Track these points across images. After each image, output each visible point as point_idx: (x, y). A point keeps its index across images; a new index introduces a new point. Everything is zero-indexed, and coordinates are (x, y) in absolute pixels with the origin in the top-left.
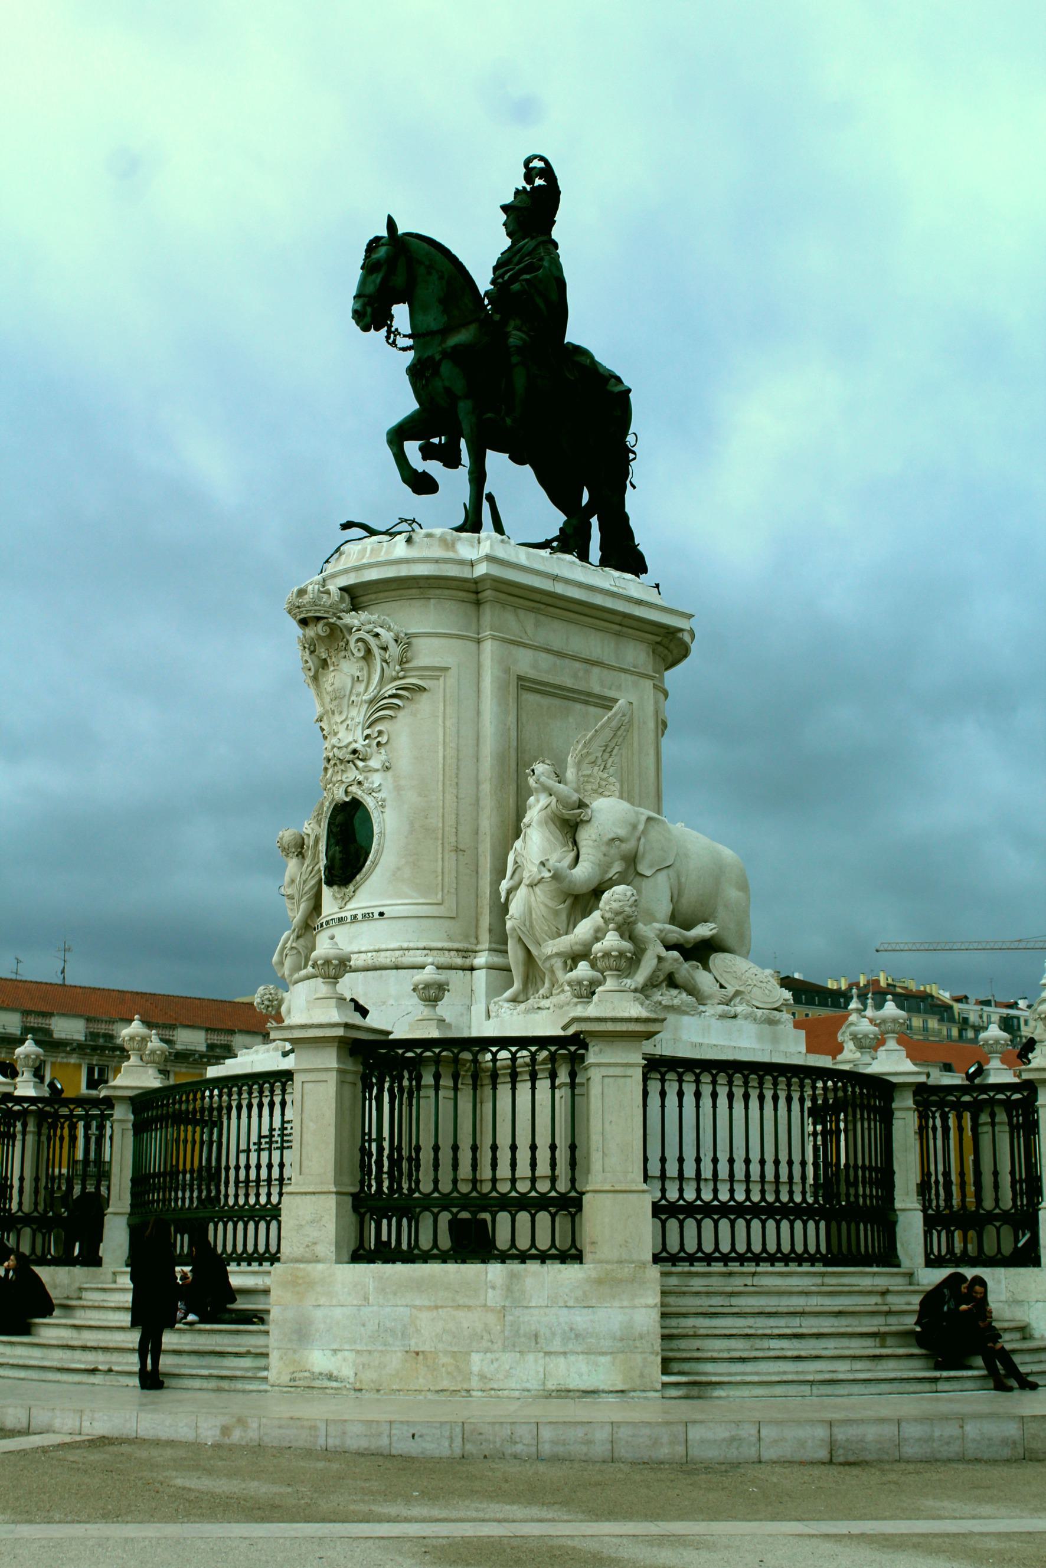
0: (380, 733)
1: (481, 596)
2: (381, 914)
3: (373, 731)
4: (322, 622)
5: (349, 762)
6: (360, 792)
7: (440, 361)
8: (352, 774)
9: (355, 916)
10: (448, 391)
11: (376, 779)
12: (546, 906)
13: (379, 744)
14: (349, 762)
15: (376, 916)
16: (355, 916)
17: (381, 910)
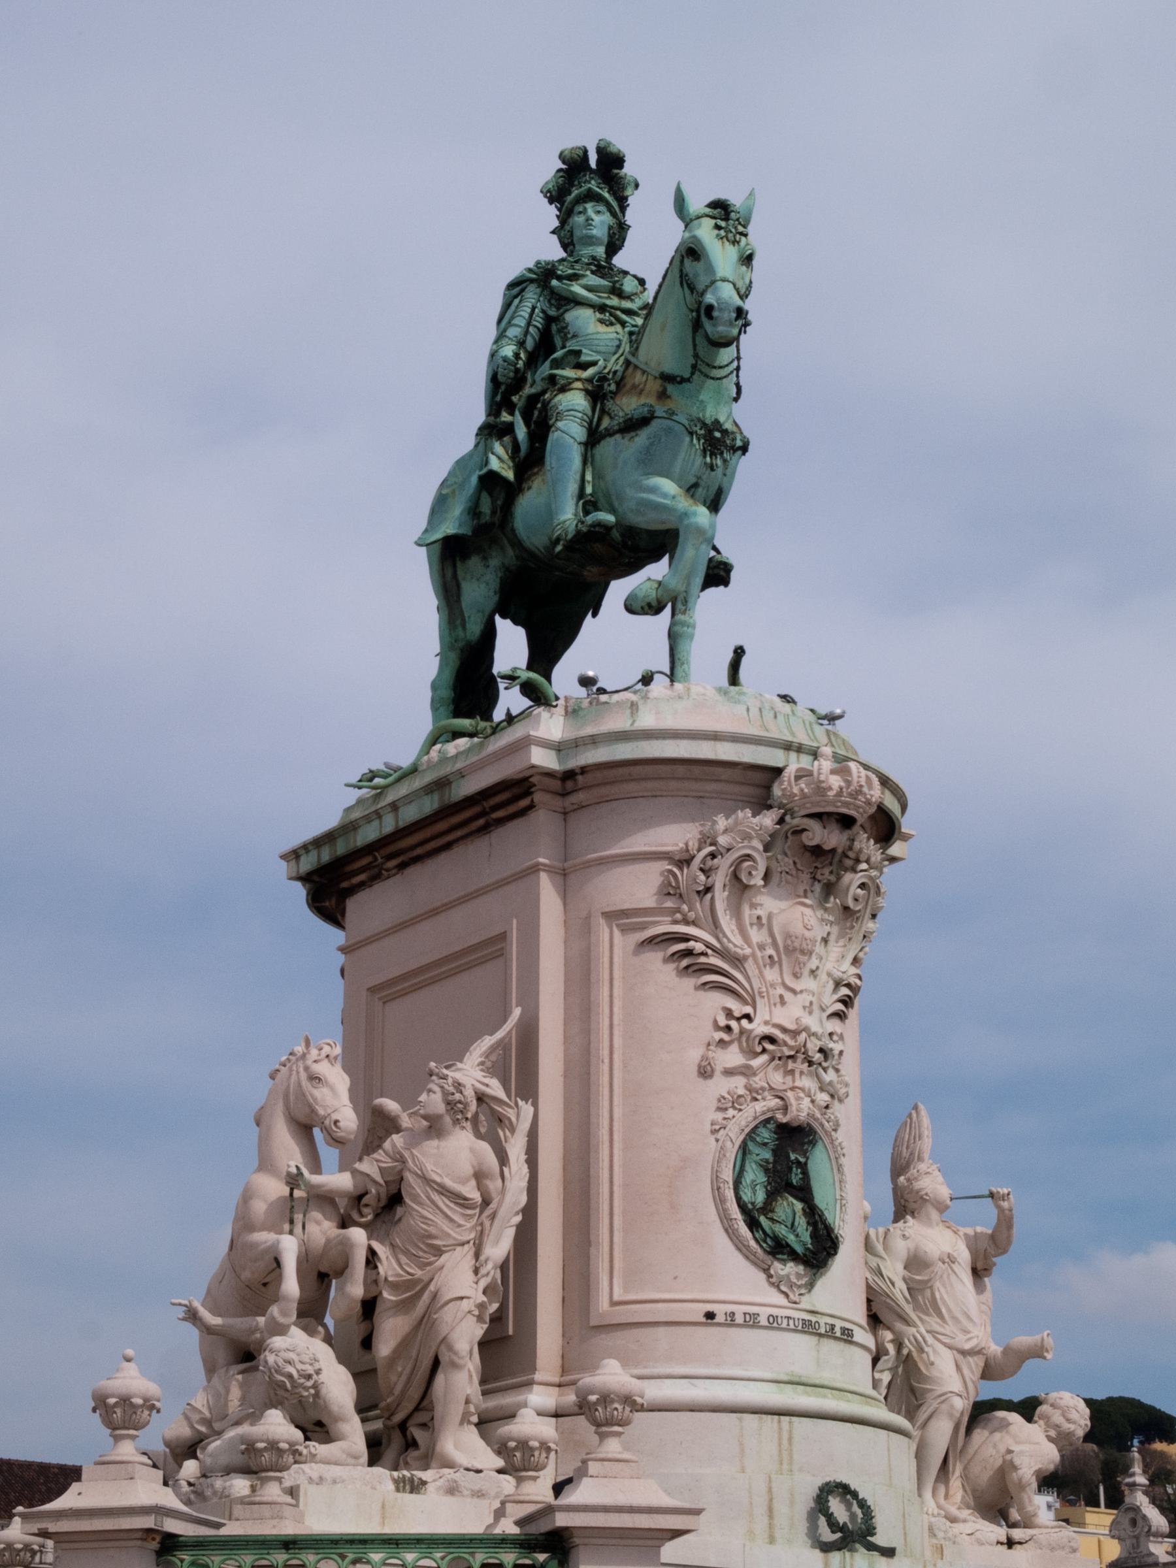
5: (811, 1063)
9: (833, 1327)
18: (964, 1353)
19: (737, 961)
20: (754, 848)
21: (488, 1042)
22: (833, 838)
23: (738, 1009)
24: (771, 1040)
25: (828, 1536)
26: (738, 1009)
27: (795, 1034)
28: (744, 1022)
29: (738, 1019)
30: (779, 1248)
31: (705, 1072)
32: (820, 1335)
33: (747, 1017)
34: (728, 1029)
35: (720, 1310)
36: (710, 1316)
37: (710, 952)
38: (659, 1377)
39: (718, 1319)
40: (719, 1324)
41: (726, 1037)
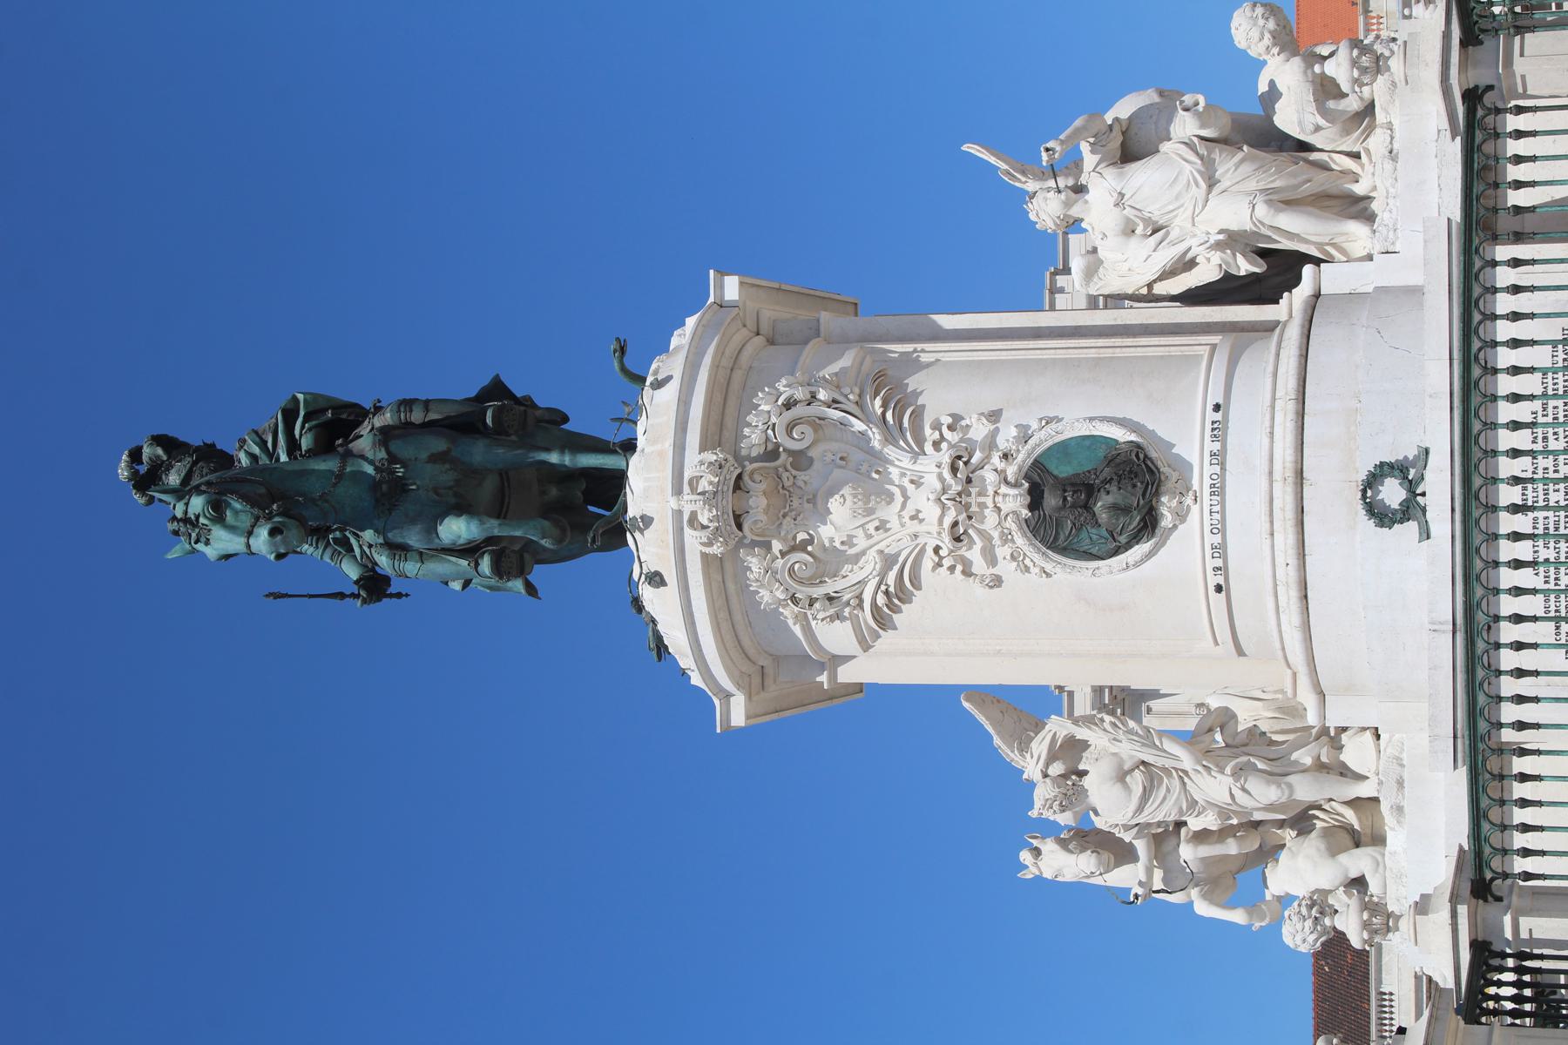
0: (937, 426)
1: (765, 327)
2: (1217, 408)
3: (930, 434)
4: (746, 478)
5: (969, 481)
6: (1020, 457)
7: (388, 452)
8: (990, 476)
9: (1212, 455)
10: (435, 458)
11: (1007, 436)
12: (1242, 161)
13: (950, 428)
14: (969, 481)
15: (1218, 416)
16: (1212, 455)
17: (1210, 407)
18: (1211, 187)
19: (889, 560)
20: (784, 565)
21: (997, 741)
22: (758, 503)
23: (929, 560)
24: (955, 524)
25: (1412, 527)
26: (929, 560)
27: (944, 508)
28: (943, 553)
29: (941, 558)
30: (1148, 524)
31: (997, 581)
32: (1223, 469)
33: (937, 550)
34: (952, 569)
35: (1213, 580)
36: (1219, 589)
37: (883, 588)
38: (1280, 632)
39: (1222, 583)
40: (1227, 579)
41: (959, 568)
